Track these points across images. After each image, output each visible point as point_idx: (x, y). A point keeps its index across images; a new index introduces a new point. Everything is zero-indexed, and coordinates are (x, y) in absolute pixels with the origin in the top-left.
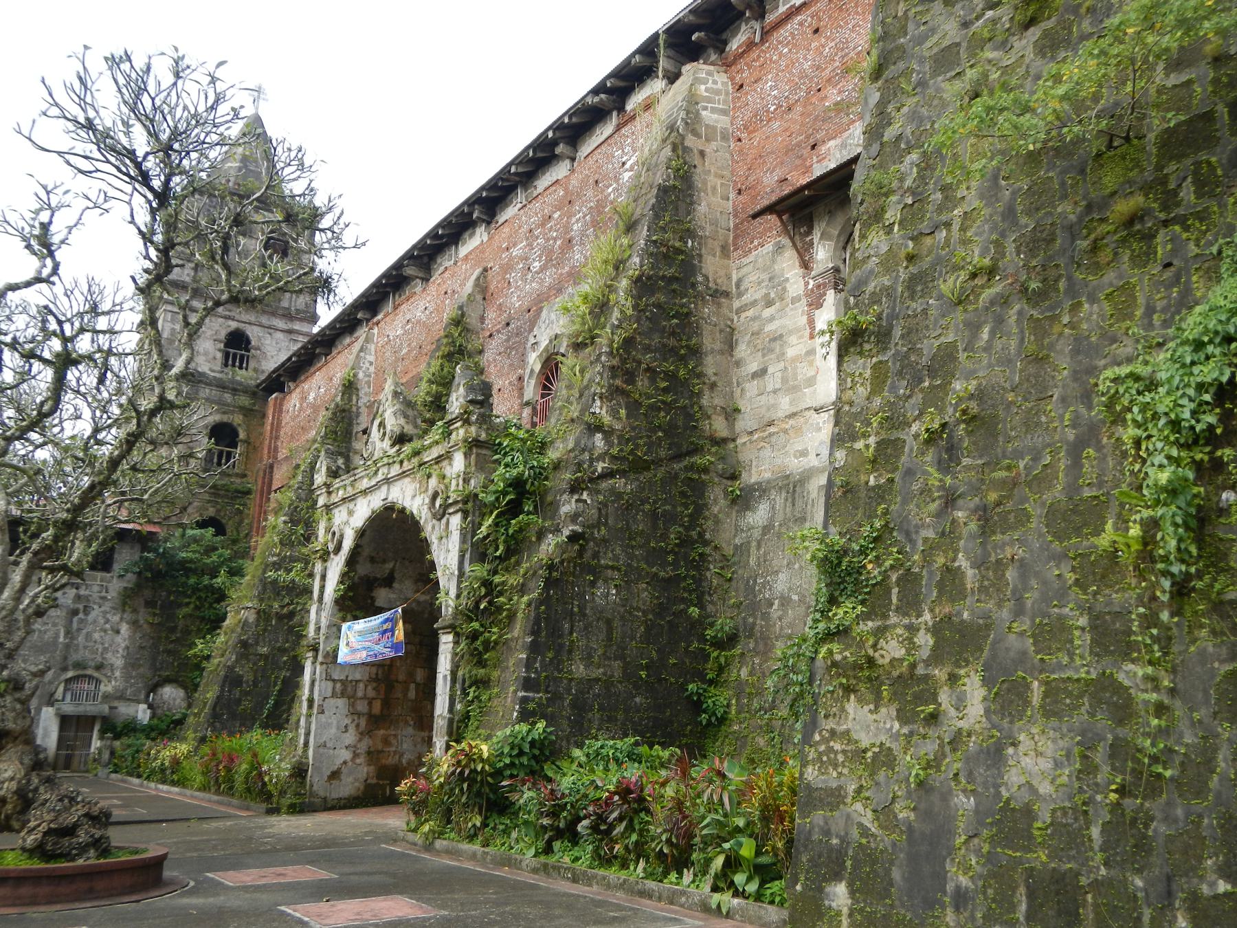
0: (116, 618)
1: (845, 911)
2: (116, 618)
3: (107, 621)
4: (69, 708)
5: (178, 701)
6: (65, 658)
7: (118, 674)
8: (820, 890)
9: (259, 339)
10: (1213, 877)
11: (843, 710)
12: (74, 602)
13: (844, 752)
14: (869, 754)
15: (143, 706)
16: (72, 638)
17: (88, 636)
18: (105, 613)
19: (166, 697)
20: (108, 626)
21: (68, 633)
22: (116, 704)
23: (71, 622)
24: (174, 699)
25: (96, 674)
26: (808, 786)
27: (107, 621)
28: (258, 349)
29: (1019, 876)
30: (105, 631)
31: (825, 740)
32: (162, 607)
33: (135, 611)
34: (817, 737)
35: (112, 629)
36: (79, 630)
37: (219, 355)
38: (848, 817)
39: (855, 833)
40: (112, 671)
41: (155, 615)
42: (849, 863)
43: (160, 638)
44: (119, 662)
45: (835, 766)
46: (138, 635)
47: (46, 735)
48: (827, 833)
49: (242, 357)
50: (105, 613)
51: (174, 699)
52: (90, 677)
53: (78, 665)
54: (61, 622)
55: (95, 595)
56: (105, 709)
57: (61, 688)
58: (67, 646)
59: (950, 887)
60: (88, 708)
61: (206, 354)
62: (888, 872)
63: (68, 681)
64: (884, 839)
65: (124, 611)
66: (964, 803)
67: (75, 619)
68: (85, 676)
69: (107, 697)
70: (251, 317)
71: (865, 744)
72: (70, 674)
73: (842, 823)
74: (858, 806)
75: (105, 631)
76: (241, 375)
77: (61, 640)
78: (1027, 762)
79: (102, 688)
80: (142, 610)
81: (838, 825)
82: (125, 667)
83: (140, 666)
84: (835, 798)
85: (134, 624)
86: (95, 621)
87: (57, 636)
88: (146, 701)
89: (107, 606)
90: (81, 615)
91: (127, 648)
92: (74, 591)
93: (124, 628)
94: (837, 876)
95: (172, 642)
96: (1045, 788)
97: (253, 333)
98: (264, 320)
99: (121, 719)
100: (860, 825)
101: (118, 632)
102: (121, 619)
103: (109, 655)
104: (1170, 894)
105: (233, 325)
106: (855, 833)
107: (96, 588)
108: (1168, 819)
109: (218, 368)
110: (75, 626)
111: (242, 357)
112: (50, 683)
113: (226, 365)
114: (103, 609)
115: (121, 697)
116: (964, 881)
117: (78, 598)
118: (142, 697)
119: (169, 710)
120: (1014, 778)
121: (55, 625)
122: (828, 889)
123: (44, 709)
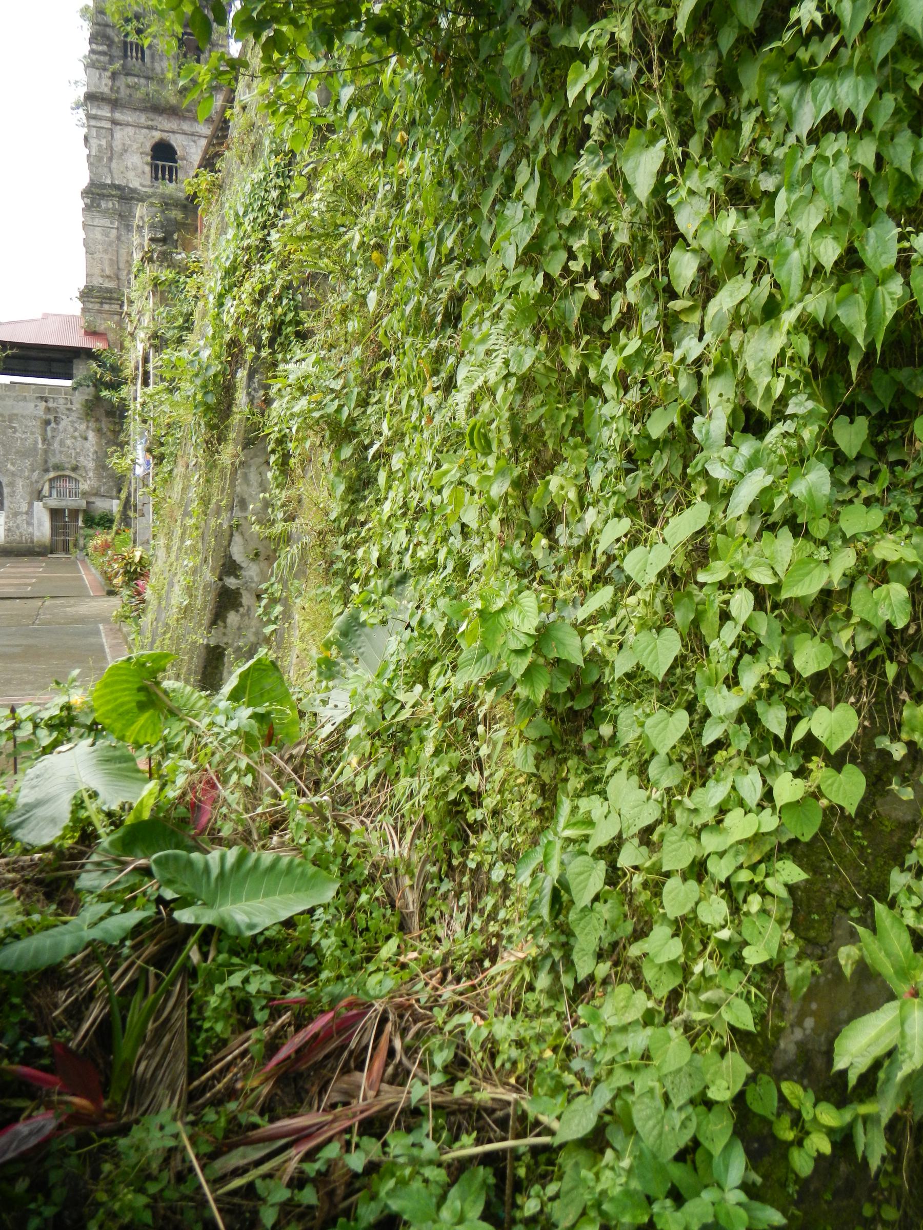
2: (83, 427)
4: (54, 503)
6: (46, 462)
7: (91, 474)
9: (184, 147)
17: (62, 443)
18: (72, 422)
21: (44, 440)
22: (93, 499)
27: (76, 430)
28: (184, 159)
33: (97, 420)
37: (147, 169)
44: (91, 465)
47: (40, 524)
49: (171, 168)
50: (72, 422)
53: (57, 467)
54: (38, 431)
55: (62, 407)
56: (83, 504)
57: (47, 487)
58: (46, 452)
61: (135, 169)
63: (51, 480)
69: (84, 494)
70: (172, 124)
72: (52, 475)
76: (170, 188)
80: (104, 420)
85: (99, 431)
87: (36, 443)
89: (74, 416)
90: (53, 425)
93: (91, 435)
97: (177, 142)
98: (186, 126)
101: (86, 439)
103: (81, 459)
105: (157, 135)
107: (62, 401)
109: (148, 183)
110: (49, 434)
111: (171, 168)
113: (156, 178)
115: (97, 494)
117: (48, 409)
121: (32, 433)
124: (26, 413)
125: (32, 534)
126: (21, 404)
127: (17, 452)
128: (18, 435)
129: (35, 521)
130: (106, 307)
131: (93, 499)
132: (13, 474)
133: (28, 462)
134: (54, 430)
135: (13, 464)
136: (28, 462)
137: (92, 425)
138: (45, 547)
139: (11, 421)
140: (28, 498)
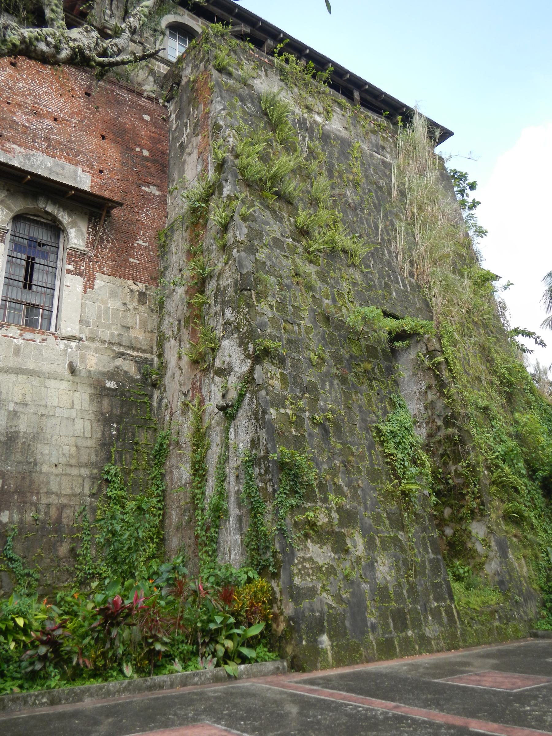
1: (329, 648)
8: (316, 640)
10: (433, 601)
11: (306, 546)
13: (312, 568)
14: (324, 569)
26: (297, 587)
29: (389, 613)
31: (300, 562)
34: (296, 561)
38: (321, 601)
39: (326, 608)
42: (326, 624)
45: (309, 576)
48: (313, 611)
59: (369, 624)
62: (343, 623)
64: (341, 608)
66: (366, 587)
71: (321, 564)
73: (319, 604)
74: (324, 595)
78: (381, 568)
81: (317, 606)
84: (312, 592)
94: (322, 632)
96: (389, 578)
100: (327, 604)
104: (426, 610)
106: (326, 608)
108: (421, 585)
116: (373, 620)
120: (379, 575)
122: (319, 639)
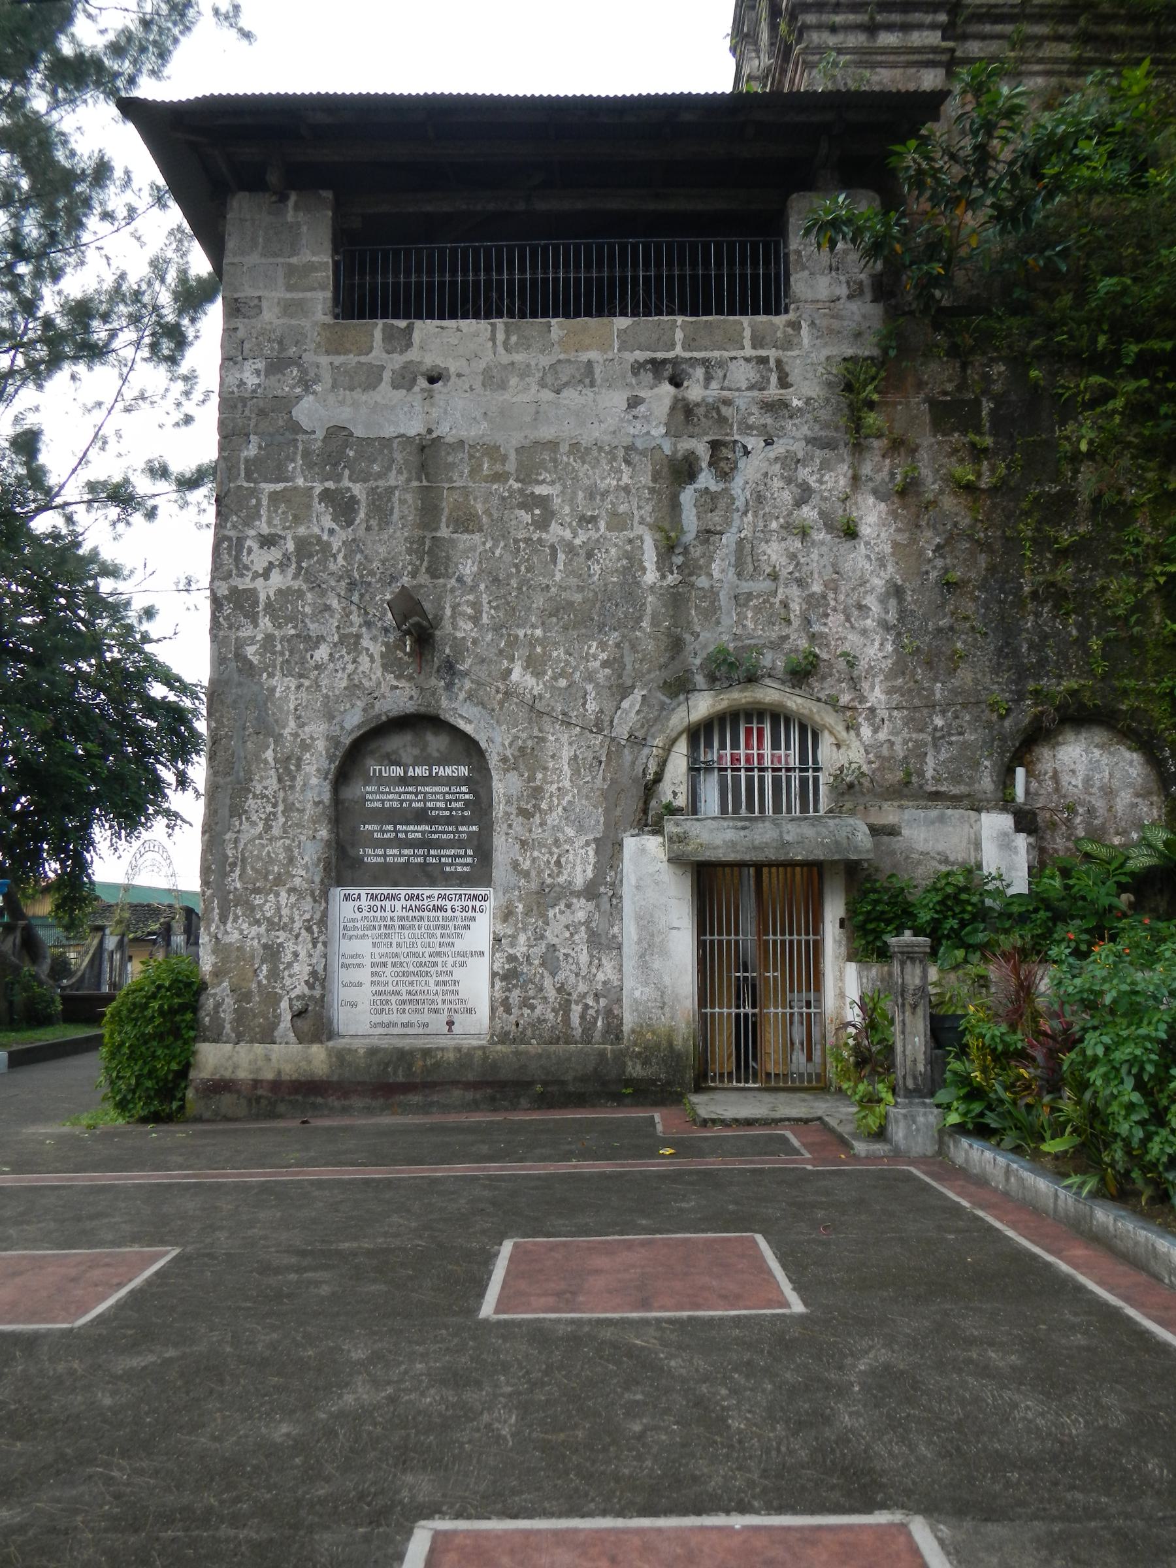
0: (837, 479)
2: (837, 479)
3: (804, 495)
5: (1124, 798)
6: (676, 645)
7: (876, 695)
12: (672, 432)
15: (995, 823)
16: (689, 569)
18: (790, 462)
19: (1073, 784)
20: (808, 513)
21: (669, 548)
22: (889, 815)
23: (675, 506)
24: (1109, 793)
25: (795, 702)
27: (804, 495)
30: (804, 533)
32: (999, 425)
35: (829, 527)
36: (708, 535)
40: (854, 683)
41: (978, 453)
43: (1012, 544)
46: (929, 540)
47: (651, 945)
50: (790, 462)
51: (1109, 793)
52: (778, 717)
54: (641, 510)
55: (743, 400)
57: (678, 763)
58: (676, 600)
60: (791, 832)
63: (699, 734)
65: (858, 450)
67: (688, 496)
68: (757, 713)
72: (703, 705)
75: (804, 533)
77: (651, 576)
79: (827, 754)
80: (927, 440)
82: (900, 668)
83: (956, 659)
86: (760, 498)
87: (633, 563)
88: (1005, 802)
90: (706, 479)
91: (896, 591)
92: (667, 389)
95: (1064, 554)
99: (923, 875)
101: (850, 533)
102: (855, 479)
103: (834, 624)
107: (742, 374)
110: (690, 519)
112: (636, 741)
114: (779, 448)
117: (684, 413)
118: (987, 783)
119: (1095, 834)
121: (619, 522)
123: (631, 843)
124: (592, 433)
125: (613, 994)
126: (571, 396)
127: (557, 609)
128: (557, 532)
129: (630, 932)
130: (888, 39)
131: (889, 815)
132: (535, 711)
133: (597, 653)
134: (709, 501)
135: (534, 665)
136: (597, 653)
137: (876, 467)
138: (673, 1057)
139: (527, 475)
140: (596, 820)
